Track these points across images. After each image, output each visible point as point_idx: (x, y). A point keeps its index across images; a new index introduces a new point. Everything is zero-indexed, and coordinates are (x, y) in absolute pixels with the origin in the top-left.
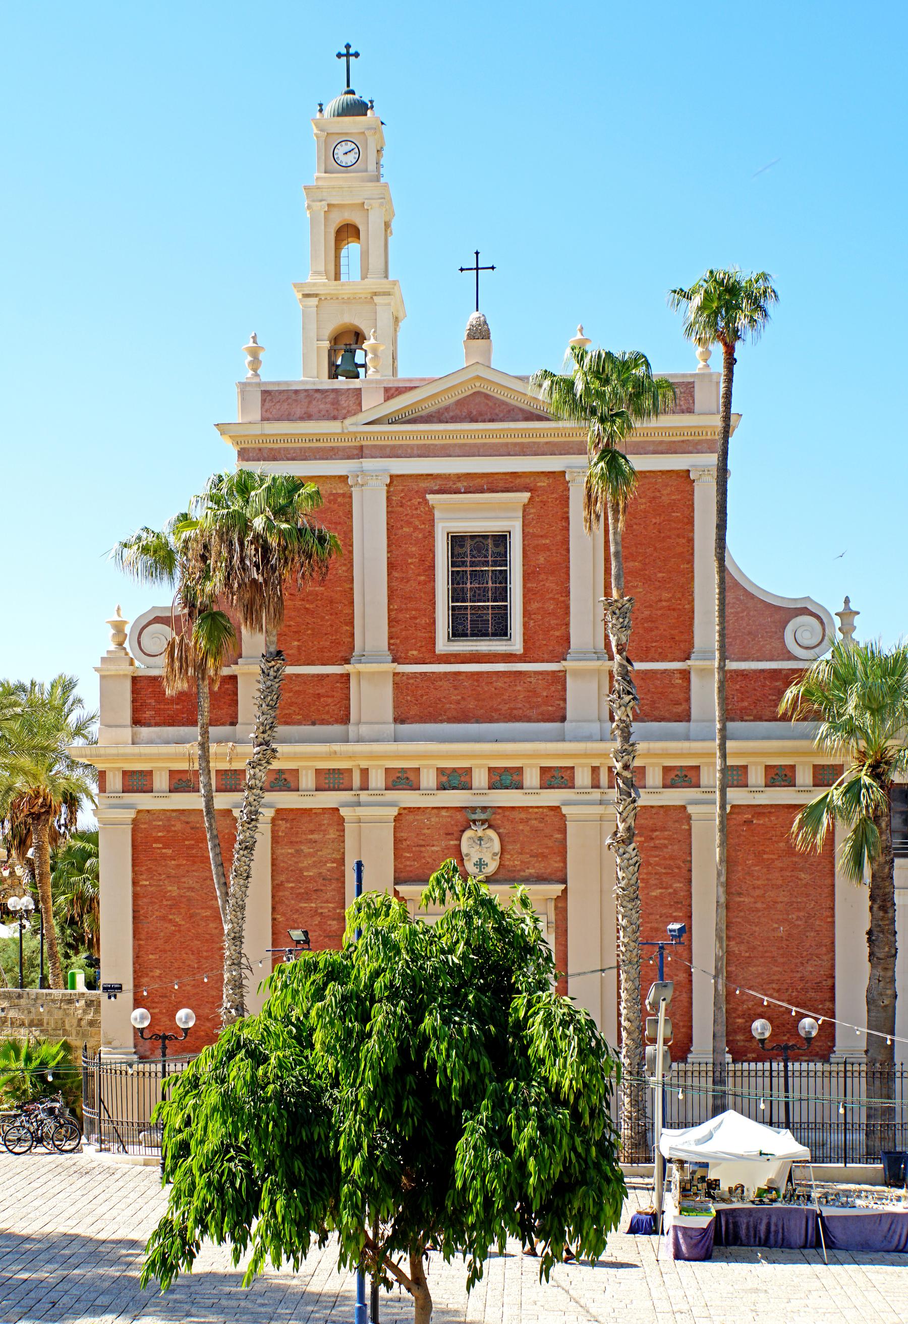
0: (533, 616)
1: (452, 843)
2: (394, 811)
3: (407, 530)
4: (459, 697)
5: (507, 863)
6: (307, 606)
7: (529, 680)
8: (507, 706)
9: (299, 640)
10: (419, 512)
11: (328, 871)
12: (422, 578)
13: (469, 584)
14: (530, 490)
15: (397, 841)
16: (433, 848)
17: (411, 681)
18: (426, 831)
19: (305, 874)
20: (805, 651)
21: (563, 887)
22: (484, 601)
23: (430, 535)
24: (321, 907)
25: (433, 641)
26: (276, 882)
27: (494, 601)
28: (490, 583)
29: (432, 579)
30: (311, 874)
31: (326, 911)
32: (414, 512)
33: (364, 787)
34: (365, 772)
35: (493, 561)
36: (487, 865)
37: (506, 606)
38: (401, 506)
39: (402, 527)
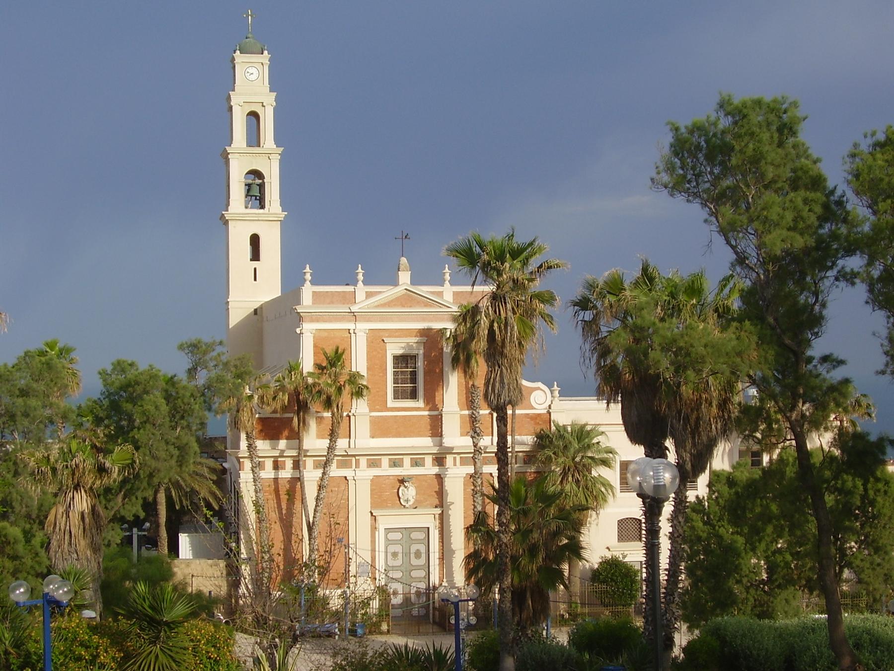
2: (371, 478)
12: (381, 374)
14: (427, 337)
33: (357, 466)
34: (357, 462)
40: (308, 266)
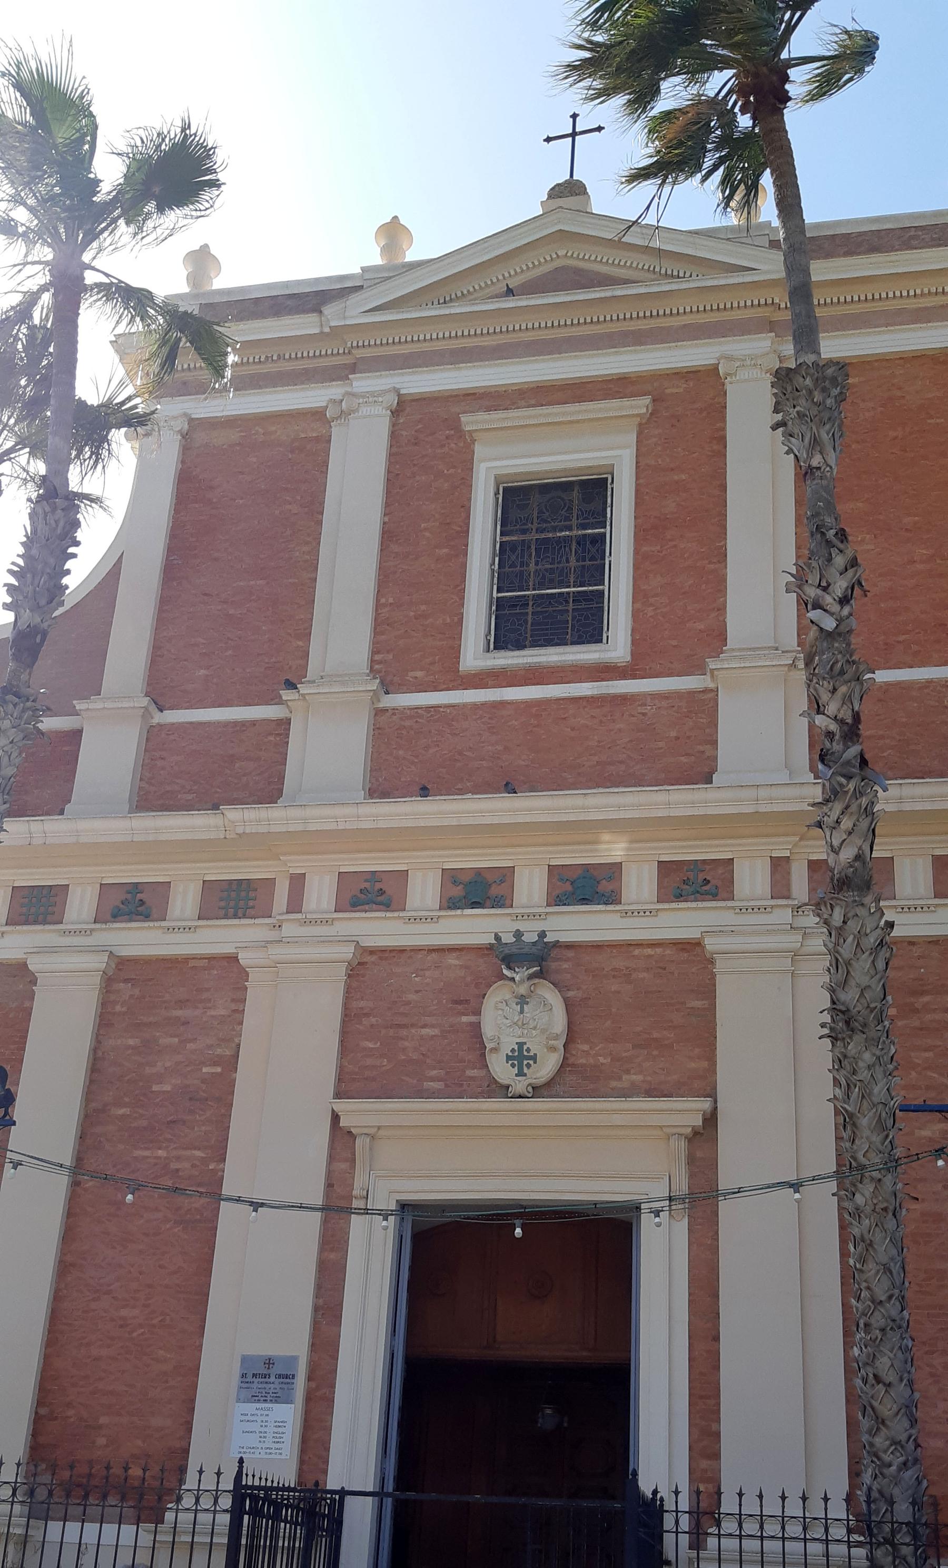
0: (652, 600)
1: (465, 1019)
2: (347, 952)
4: (500, 748)
5: (583, 1061)
6: (231, 612)
7: (640, 709)
8: (596, 758)
9: (208, 668)
11: (204, 1081)
13: (532, 567)
15: (349, 1017)
16: (425, 1031)
17: (407, 723)
18: (412, 997)
19: (155, 1088)
21: (706, 1104)
22: (561, 584)
23: (465, 483)
24: (178, 1158)
25: (455, 653)
26: (93, 1105)
28: (573, 558)
30: (167, 1088)
31: (186, 1165)
32: (439, 451)
33: (295, 904)
34: (298, 882)
36: (534, 1058)
37: (602, 592)
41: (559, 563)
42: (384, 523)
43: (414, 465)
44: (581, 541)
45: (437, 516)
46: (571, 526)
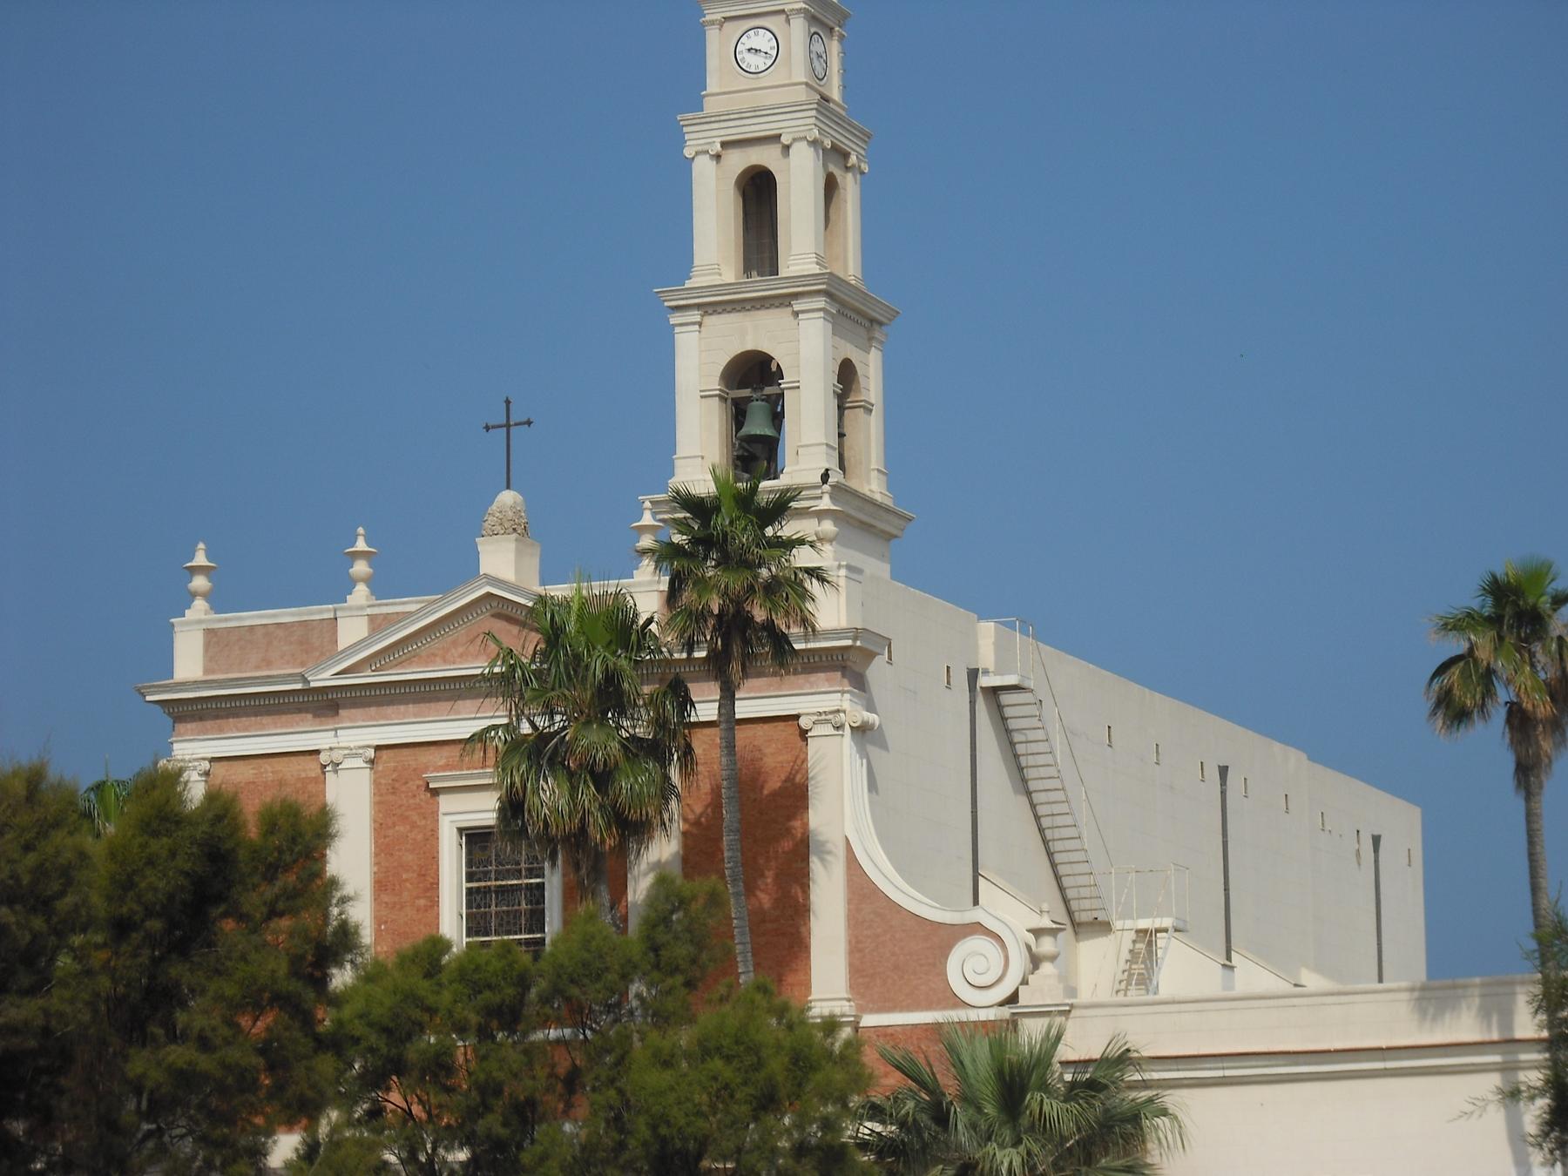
3: (402, 829)
10: (418, 801)
12: (422, 902)
13: (493, 907)
20: (977, 992)
23: (433, 835)
27: (528, 934)
28: (523, 903)
29: (434, 903)
32: (411, 801)
35: (527, 869)
38: (393, 793)
39: (394, 825)
40: (201, 546)
41: (513, 906)
42: (375, 873)
43: (394, 815)
44: (529, 887)
45: (415, 868)
46: (520, 871)
